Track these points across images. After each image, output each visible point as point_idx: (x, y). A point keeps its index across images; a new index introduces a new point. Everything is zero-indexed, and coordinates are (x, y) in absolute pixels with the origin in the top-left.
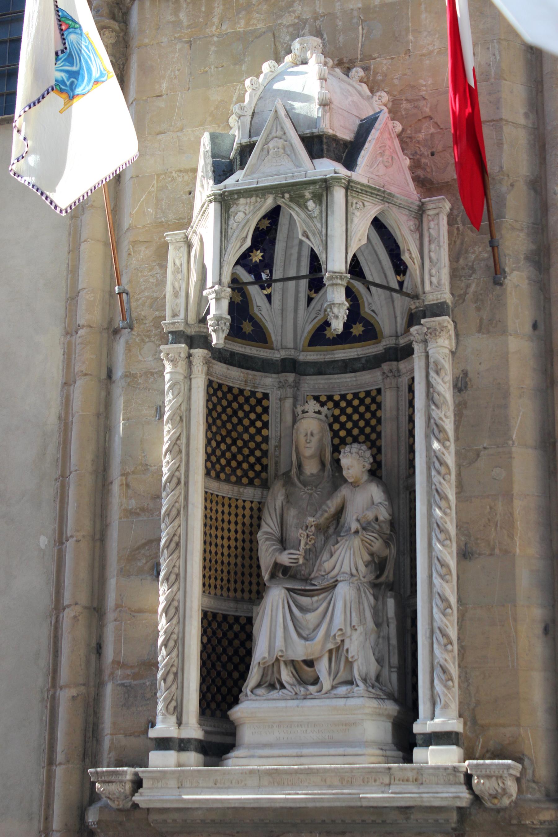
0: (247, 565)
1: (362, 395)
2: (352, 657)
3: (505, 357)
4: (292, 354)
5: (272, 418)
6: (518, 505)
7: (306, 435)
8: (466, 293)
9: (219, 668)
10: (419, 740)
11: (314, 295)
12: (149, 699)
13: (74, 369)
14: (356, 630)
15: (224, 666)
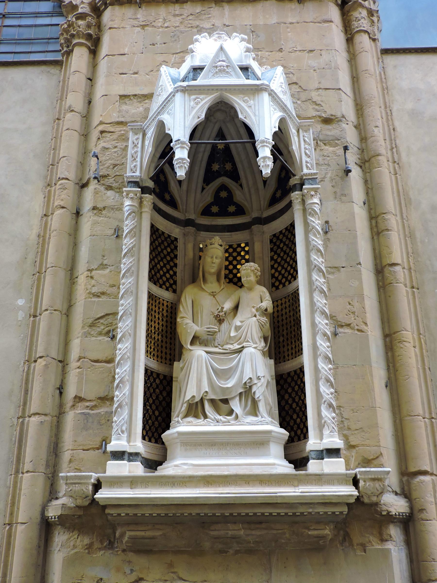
1: (235, 246)
2: (258, 398)
3: (353, 215)
4: (192, 217)
5: (180, 253)
7: (212, 257)
8: (325, 177)
10: (313, 455)
11: (205, 187)
13: (53, 203)
14: (260, 379)
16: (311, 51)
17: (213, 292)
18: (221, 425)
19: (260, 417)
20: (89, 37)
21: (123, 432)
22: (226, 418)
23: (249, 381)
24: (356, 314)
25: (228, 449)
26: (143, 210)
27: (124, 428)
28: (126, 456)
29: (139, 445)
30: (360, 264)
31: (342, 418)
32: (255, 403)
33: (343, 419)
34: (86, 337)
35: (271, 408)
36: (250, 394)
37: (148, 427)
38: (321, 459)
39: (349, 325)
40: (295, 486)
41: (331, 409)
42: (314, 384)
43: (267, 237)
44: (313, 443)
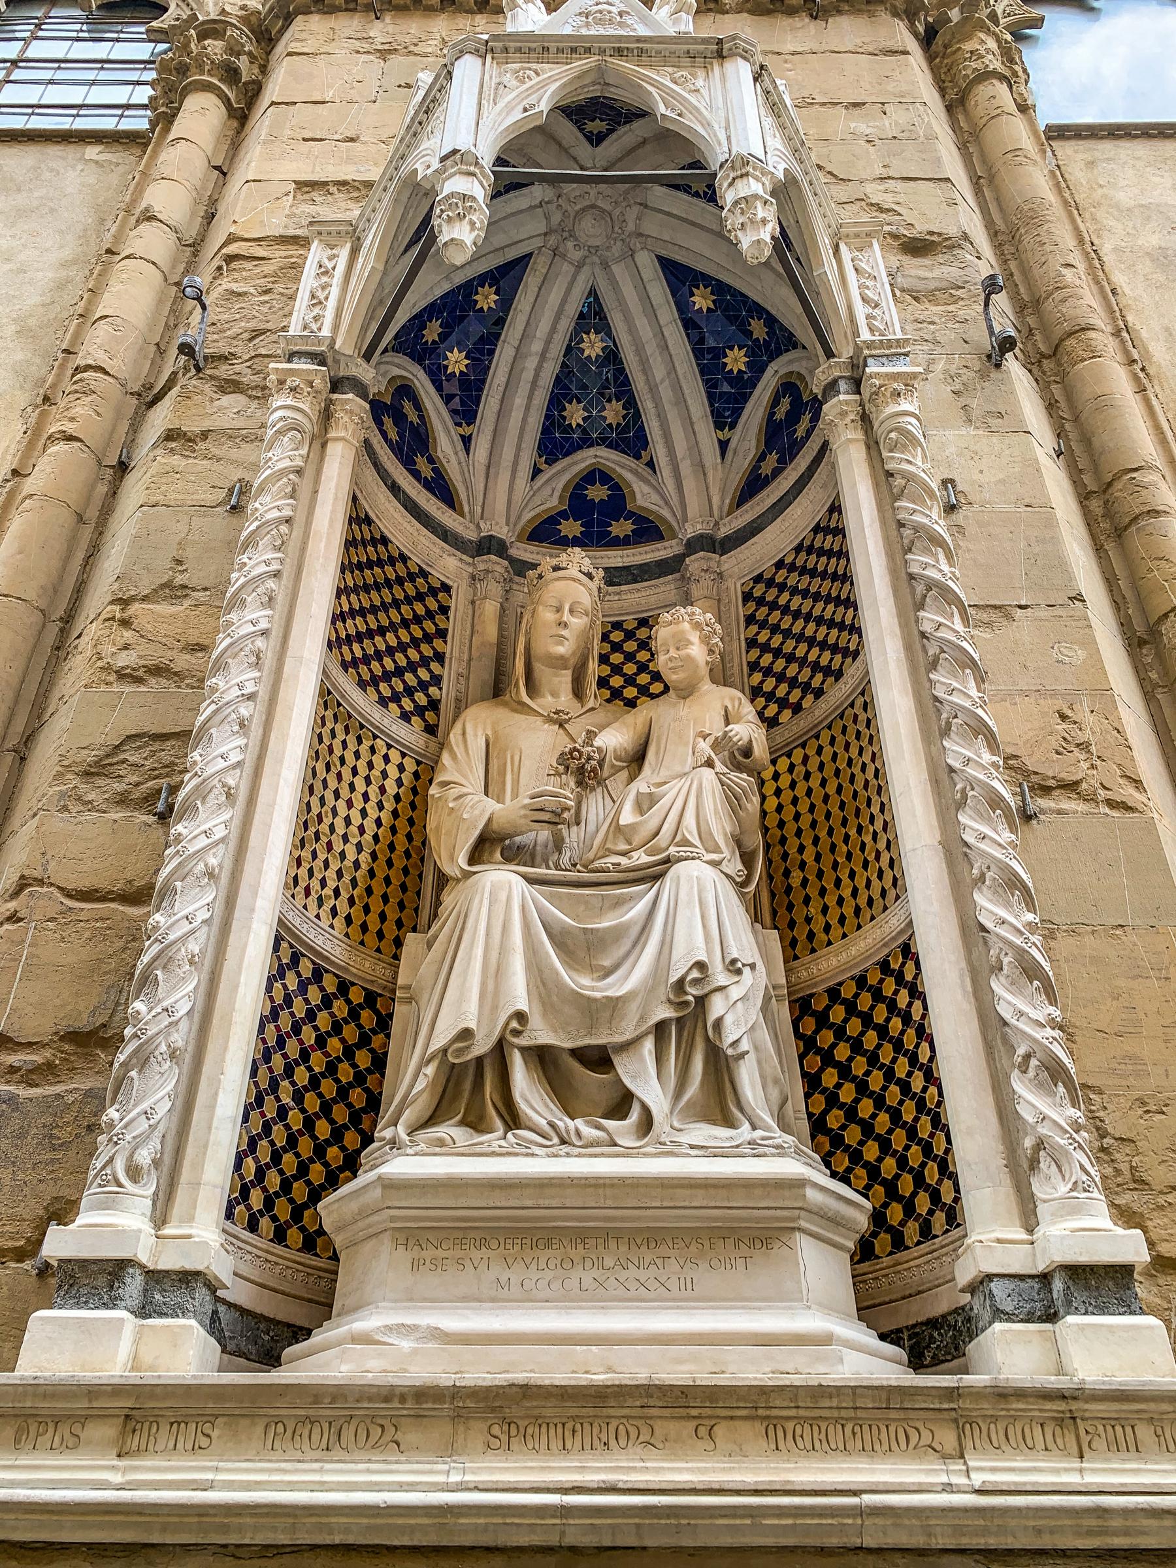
0: (380, 875)
2: (735, 1043)
4: (502, 531)
5: (457, 623)
7: (559, 610)
9: (287, 1100)
11: (544, 467)
12: (65, 1145)
14: (739, 972)
15: (298, 1097)
16: (855, 105)
17: (557, 712)
18: (579, 1155)
19: (746, 1126)
20: (231, 74)
21: (134, 1173)
22: (599, 1127)
23: (695, 974)
24: (1093, 749)
25: (609, 1262)
26: (332, 434)
27: (144, 1157)
28: (133, 1285)
29: (201, 1236)
30: (1079, 598)
31: (1102, 1137)
32: (720, 1066)
33: (1107, 1141)
34: (65, 808)
35: (784, 1102)
36: (699, 1031)
37: (278, 1180)
38: (1041, 1320)
39: (1071, 787)
40: (945, 1457)
41: (1061, 1089)
42: (969, 988)
43: (735, 588)
44: (991, 1241)
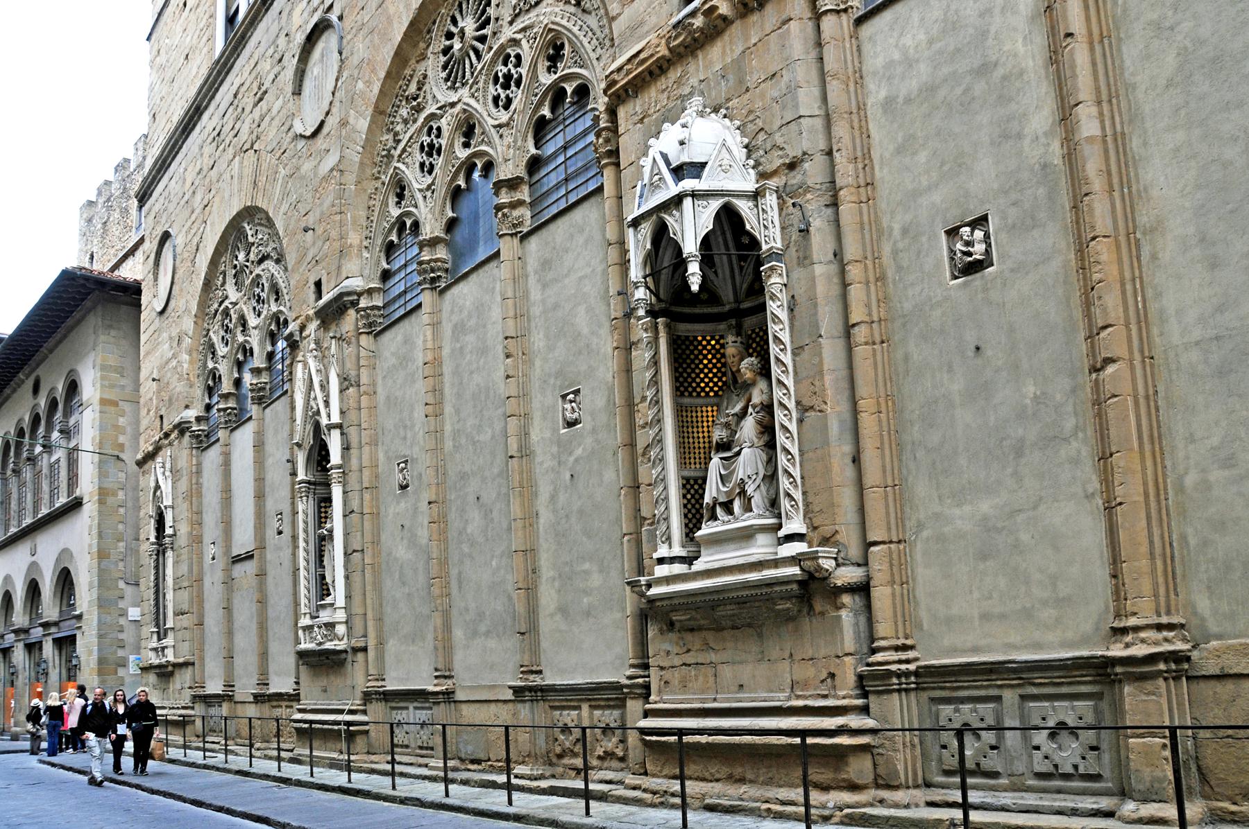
6: (828, 379)
